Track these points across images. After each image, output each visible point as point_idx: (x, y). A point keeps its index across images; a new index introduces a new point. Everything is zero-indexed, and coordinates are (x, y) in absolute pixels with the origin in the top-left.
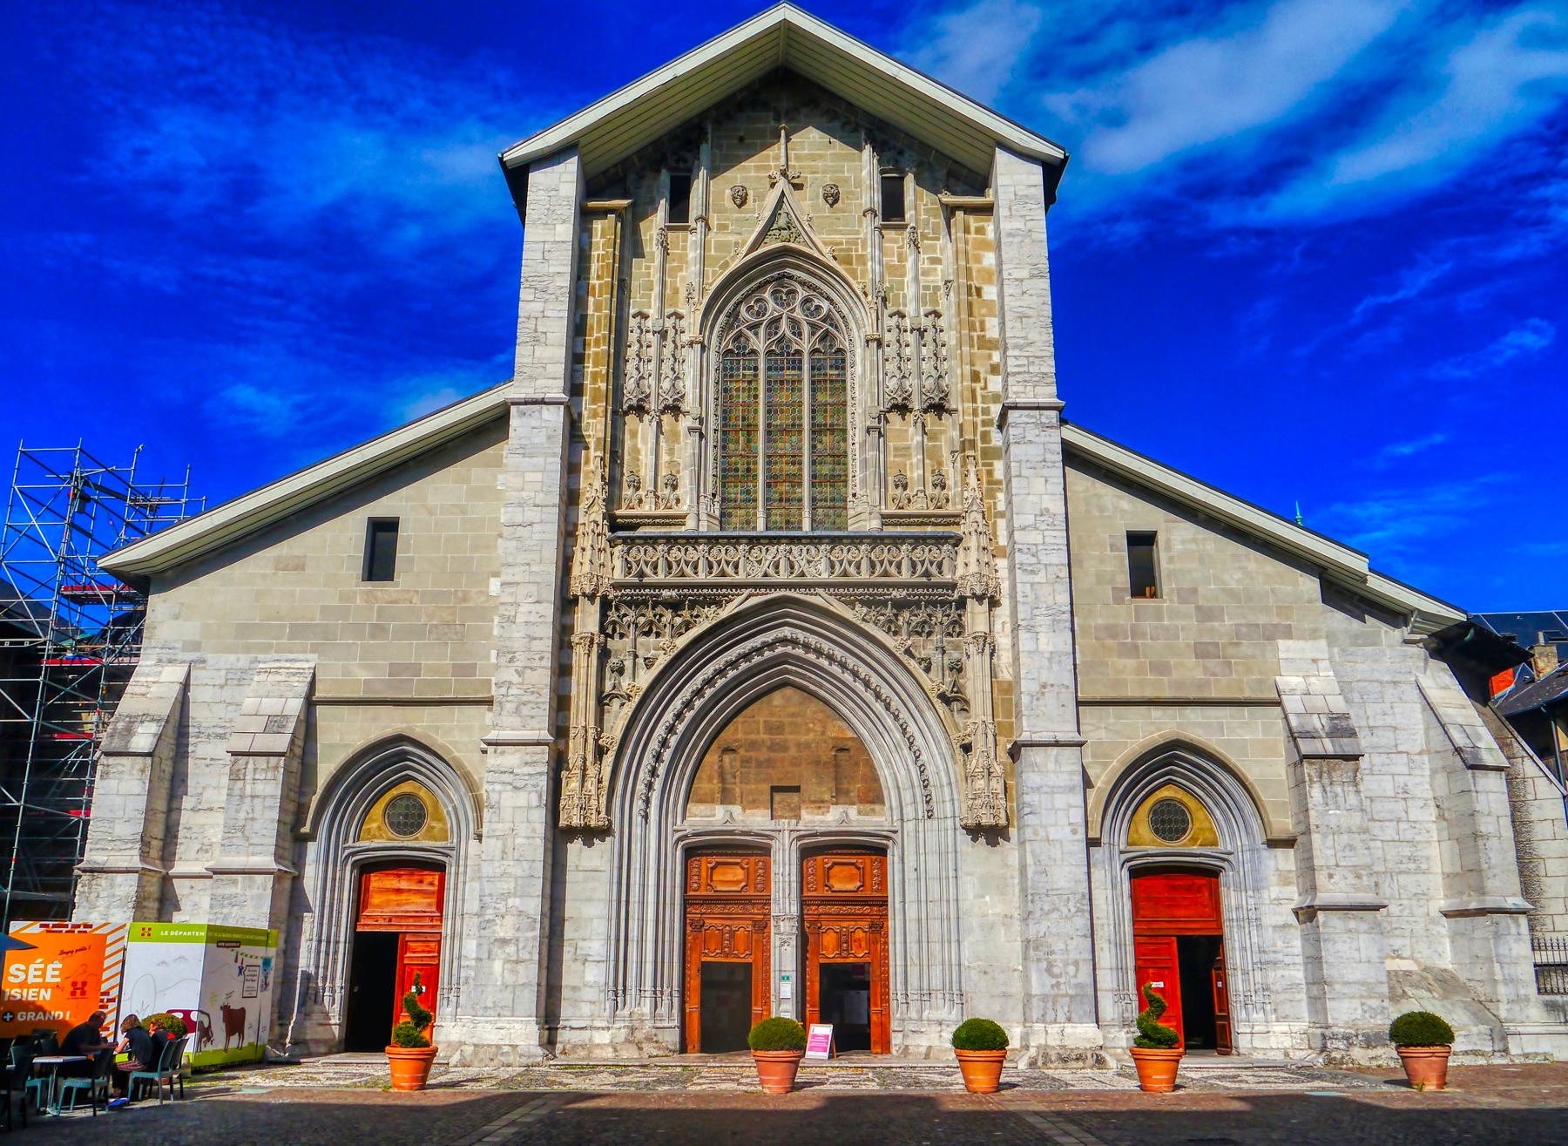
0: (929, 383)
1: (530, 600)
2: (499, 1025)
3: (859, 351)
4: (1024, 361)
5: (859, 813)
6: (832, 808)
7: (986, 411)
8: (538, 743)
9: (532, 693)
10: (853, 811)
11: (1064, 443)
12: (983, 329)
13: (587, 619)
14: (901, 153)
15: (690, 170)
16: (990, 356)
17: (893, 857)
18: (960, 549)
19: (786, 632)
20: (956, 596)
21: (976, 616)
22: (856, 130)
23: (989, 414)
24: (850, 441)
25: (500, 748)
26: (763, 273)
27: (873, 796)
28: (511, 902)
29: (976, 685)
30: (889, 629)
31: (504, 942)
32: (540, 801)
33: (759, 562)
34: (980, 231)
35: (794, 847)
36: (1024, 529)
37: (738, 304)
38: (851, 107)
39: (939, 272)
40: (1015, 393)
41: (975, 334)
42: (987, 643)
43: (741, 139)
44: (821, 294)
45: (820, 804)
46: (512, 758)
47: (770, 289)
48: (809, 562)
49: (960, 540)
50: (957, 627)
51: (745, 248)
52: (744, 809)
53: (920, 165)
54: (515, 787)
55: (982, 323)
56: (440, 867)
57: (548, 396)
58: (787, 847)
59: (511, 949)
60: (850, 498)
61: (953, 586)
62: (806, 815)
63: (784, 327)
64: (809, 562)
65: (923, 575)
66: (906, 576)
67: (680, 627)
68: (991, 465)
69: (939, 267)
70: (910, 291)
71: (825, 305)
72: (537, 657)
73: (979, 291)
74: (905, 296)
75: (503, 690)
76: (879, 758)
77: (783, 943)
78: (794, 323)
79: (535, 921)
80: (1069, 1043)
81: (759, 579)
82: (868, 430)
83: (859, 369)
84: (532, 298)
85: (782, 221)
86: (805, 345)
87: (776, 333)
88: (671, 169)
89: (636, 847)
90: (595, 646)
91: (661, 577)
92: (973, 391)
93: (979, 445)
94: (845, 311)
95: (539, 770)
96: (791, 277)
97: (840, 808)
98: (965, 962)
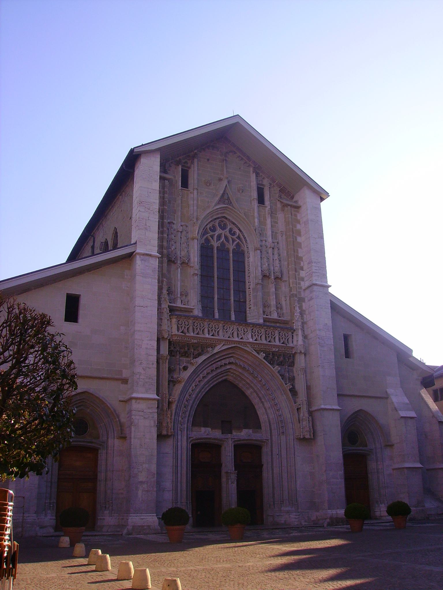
0: (277, 269)
1: (147, 339)
2: (142, 517)
3: (252, 254)
4: (317, 269)
5: (253, 432)
6: (243, 430)
7: (300, 284)
8: (154, 399)
9: (150, 378)
10: (251, 431)
11: (330, 300)
12: (297, 252)
13: (165, 350)
14: (264, 178)
15: (189, 168)
16: (300, 264)
17: (265, 450)
18: (294, 335)
19: (232, 360)
20: (293, 353)
21: (300, 361)
22: (249, 166)
23: (300, 285)
24: (247, 287)
25: (138, 401)
26: (218, 214)
27: (257, 425)
28: (144, 465)
29: (300, 386)
30: (270, 362)
31: (142, 482)
32: (155, 422)
33: (227, 332)
34: (296, 215)
35: (233, 445)
36: (320, 330)
37: (207, 225)
38: (249, 158)
39: (277, 226)
40: (316, 280)
41: (295, 254)
42: (305, 371)
43: (208, 160)
44: (237, 228)
45: (240, 429)
46: (142, 406)
47: (218, 220)
48: (244, 334)
49: (294, 330)
50: (292, 364)
51: (214, 204)
52: (212, 430)
53: (270, 184)
54: (144, 418)
55: (297, 250)
56: (95, 451)
57: (152, 253)
58: (230, 445)
59: (145, 486)
60: (248, 309)
61: (292, 348)
62: (234, 433)
63: (223, 238)
64: (244, 334)
65: (283, 343)
66: (277, 343)
67: (196, 355)
68: (302, 304)
69: (277, 225)
70: (269, 233)
71: (238, 232)
72: (151, 363)
73: (296, 237)
74: (266, 235)
75: (138, 376)
76: (260, 412)
77: (232, 483)
78: (226, 238)
79: (154, 474)
80: (338, 516)
81: (227, 339)
82: (257, 284)
83: (251, 259)
84: (144, 211)
85: (226, 197)
86: (231, 247)
87: (219, 240)
88: (182, 166)
89: (179, 444)
90: (167, 361)
91: (192, 334)
92: (296, 275)
93: (298, 296)
94: (246, 236)
95: (154, 411)
96: (226, 218)
97: (247, 430)
98: (298, 489)
